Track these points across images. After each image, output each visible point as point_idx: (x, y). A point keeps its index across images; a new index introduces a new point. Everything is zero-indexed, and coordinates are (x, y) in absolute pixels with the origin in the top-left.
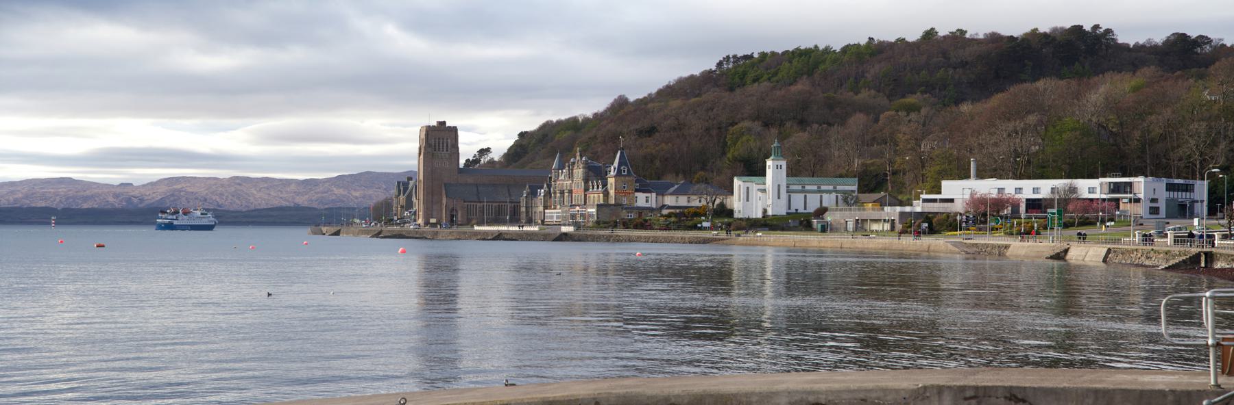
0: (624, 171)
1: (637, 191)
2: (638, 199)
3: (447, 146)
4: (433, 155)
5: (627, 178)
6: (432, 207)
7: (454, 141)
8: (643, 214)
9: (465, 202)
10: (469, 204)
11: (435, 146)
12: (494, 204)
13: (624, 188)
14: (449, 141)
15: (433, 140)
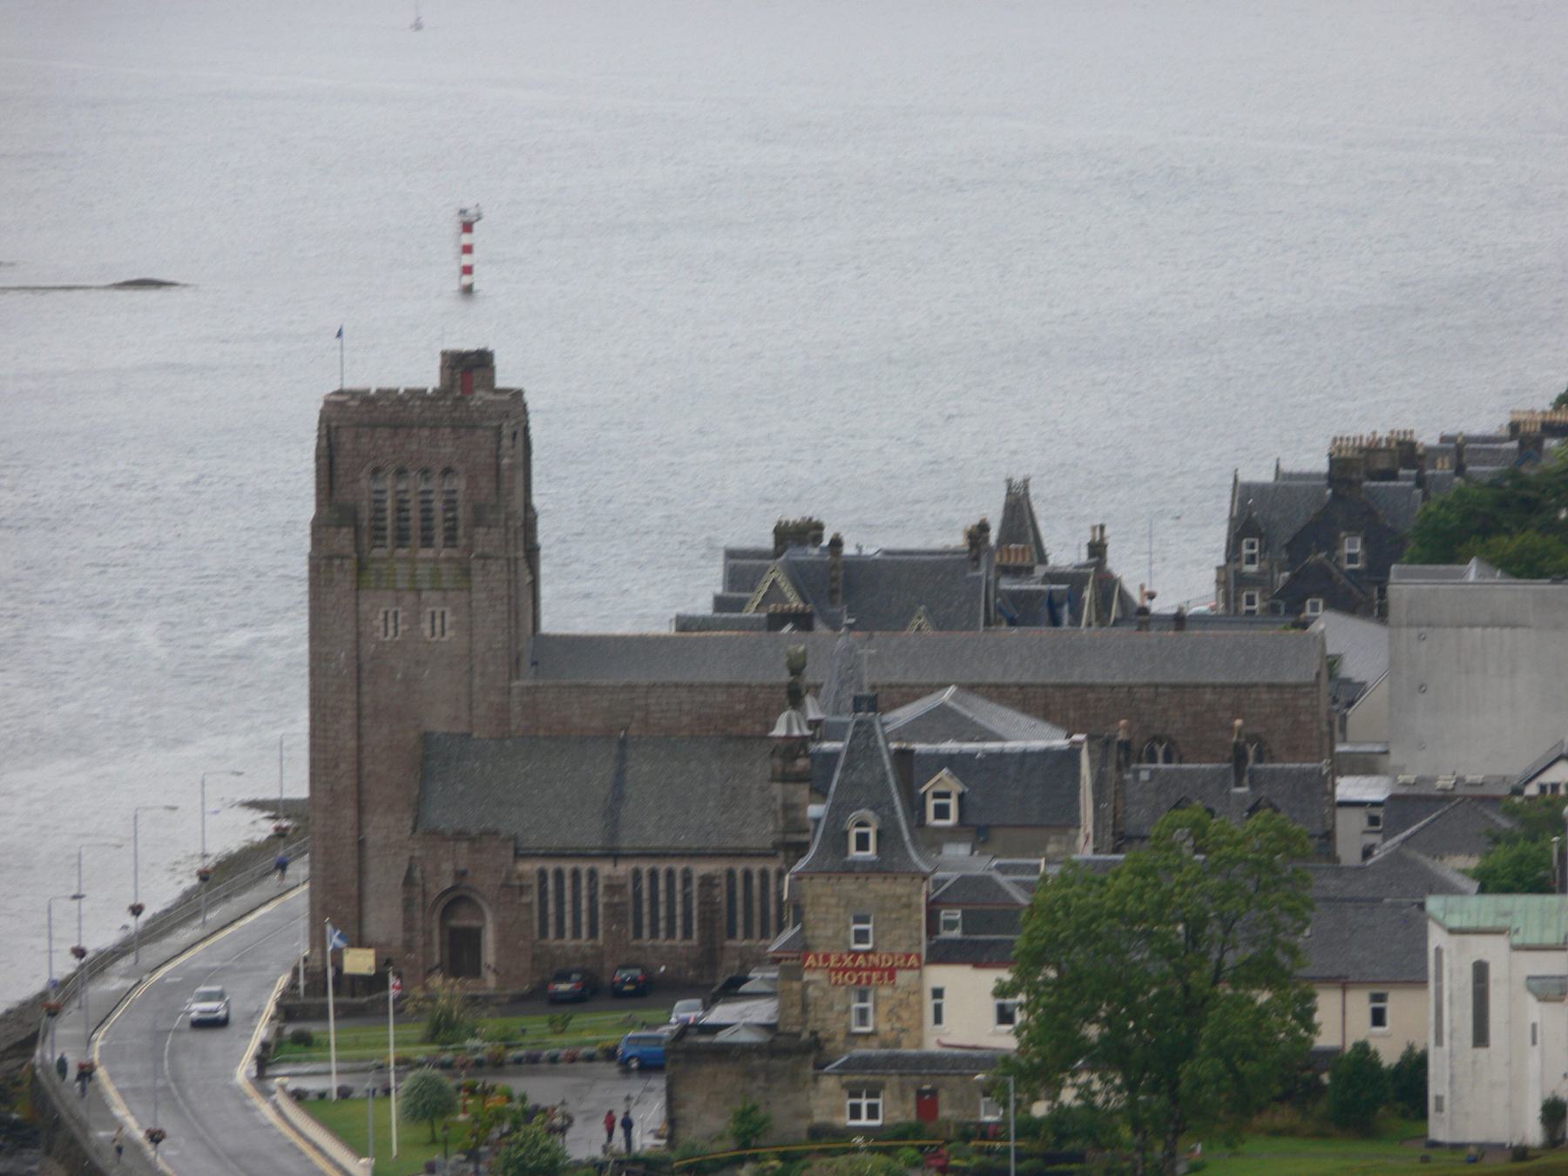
0: (862, 843)
1: (943, 954)
2: (947, 1003)
4: (361, 568)
5: (879, 886)
8: (943, 1096)
9: (520, 855)
10: (550, 866)
12: (701, 868)
13: (861, 936)
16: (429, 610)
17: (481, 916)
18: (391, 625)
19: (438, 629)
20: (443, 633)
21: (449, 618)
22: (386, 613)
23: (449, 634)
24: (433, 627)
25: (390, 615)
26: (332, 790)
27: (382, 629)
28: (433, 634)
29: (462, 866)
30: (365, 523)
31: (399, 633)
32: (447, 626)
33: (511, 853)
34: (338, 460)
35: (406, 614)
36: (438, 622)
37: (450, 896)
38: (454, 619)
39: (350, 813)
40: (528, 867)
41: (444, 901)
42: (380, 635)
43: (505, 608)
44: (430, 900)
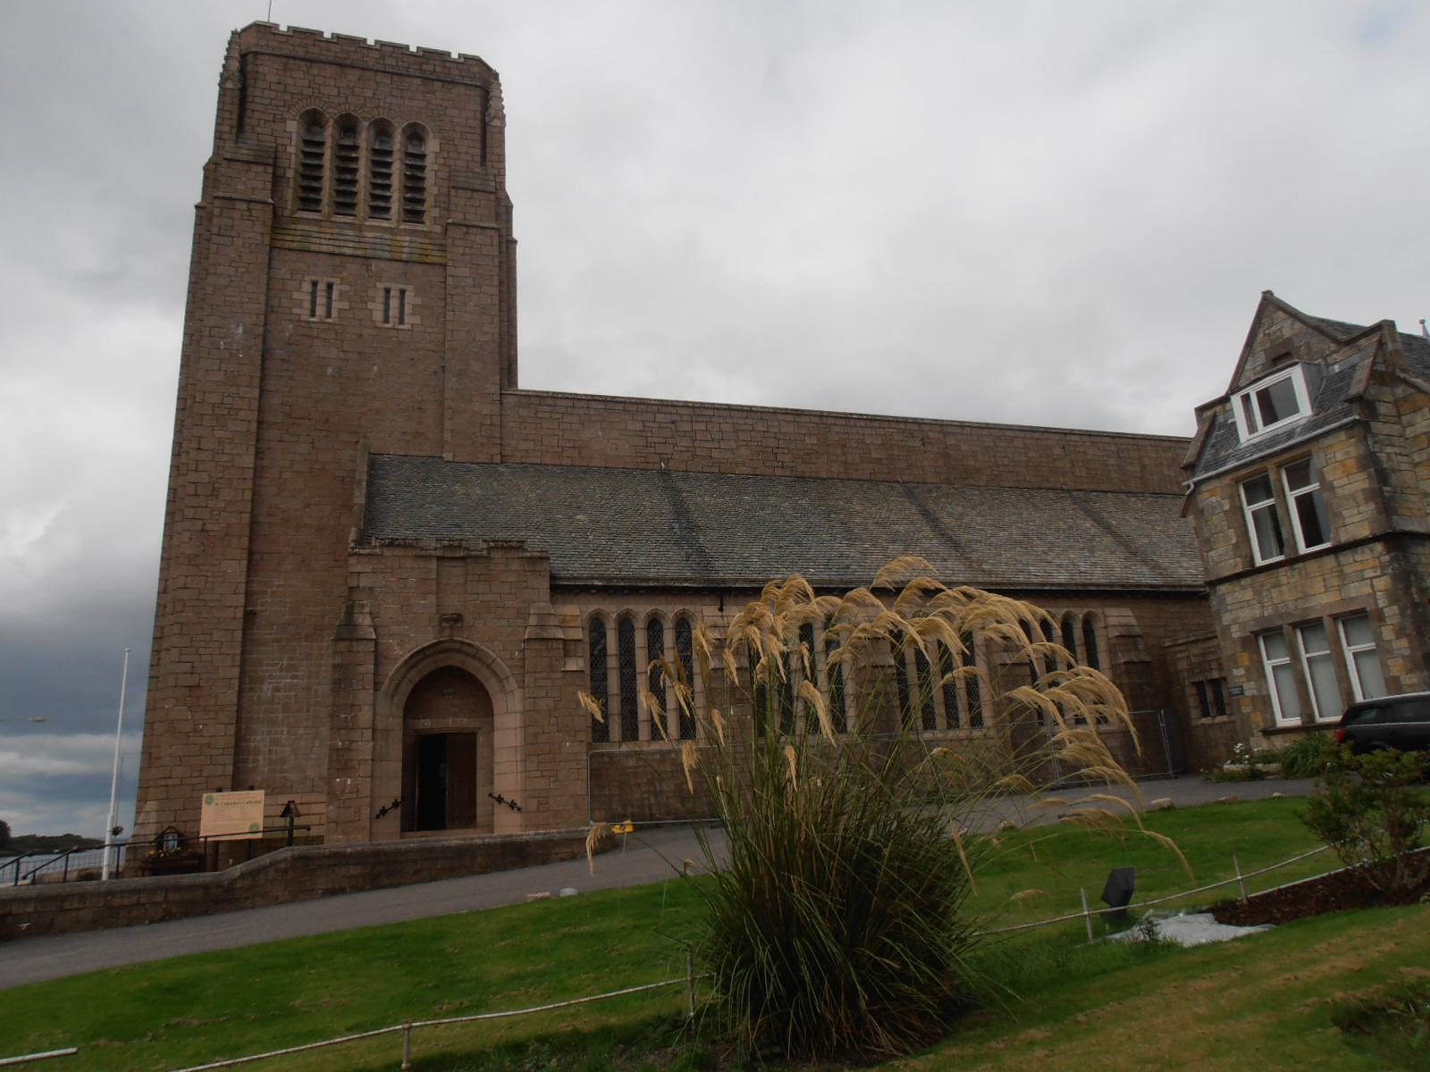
3: (414, 182)
6: (247, 680)
7: (469, 148)
9: (561, 589)
10: (612, 609)
11: (310, 172)
14: (432, 146)
15: (292, 126)
16: (380, 285)
17: (483, 704)
18: (321, 300)
19: (393, 312)
20: (402, 321)
21: (410, 298)
22: (315, 284)
23: (407, 319)
24: (387, 311)
25: (321, 287)
26: (202, 531)
27: (307, 305)
28: (386, 320)
29: (453, 604)
30: (290, 174)
31: (334, 313)
32: (407, 309)
33: (546, 584)
34: (250, 91)
35: (345, 288)
36: (394, 303)
37: (427, 666)
38: (418, 301)
39: (235, 568)
40: (576, 611)
41: (415, 676)
42: (304, 313)
43: (496, 291)
44: (391, 670)
